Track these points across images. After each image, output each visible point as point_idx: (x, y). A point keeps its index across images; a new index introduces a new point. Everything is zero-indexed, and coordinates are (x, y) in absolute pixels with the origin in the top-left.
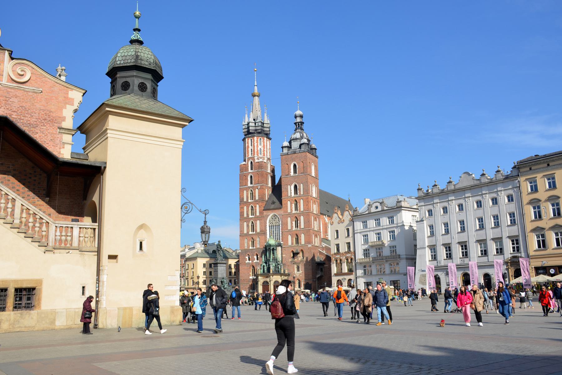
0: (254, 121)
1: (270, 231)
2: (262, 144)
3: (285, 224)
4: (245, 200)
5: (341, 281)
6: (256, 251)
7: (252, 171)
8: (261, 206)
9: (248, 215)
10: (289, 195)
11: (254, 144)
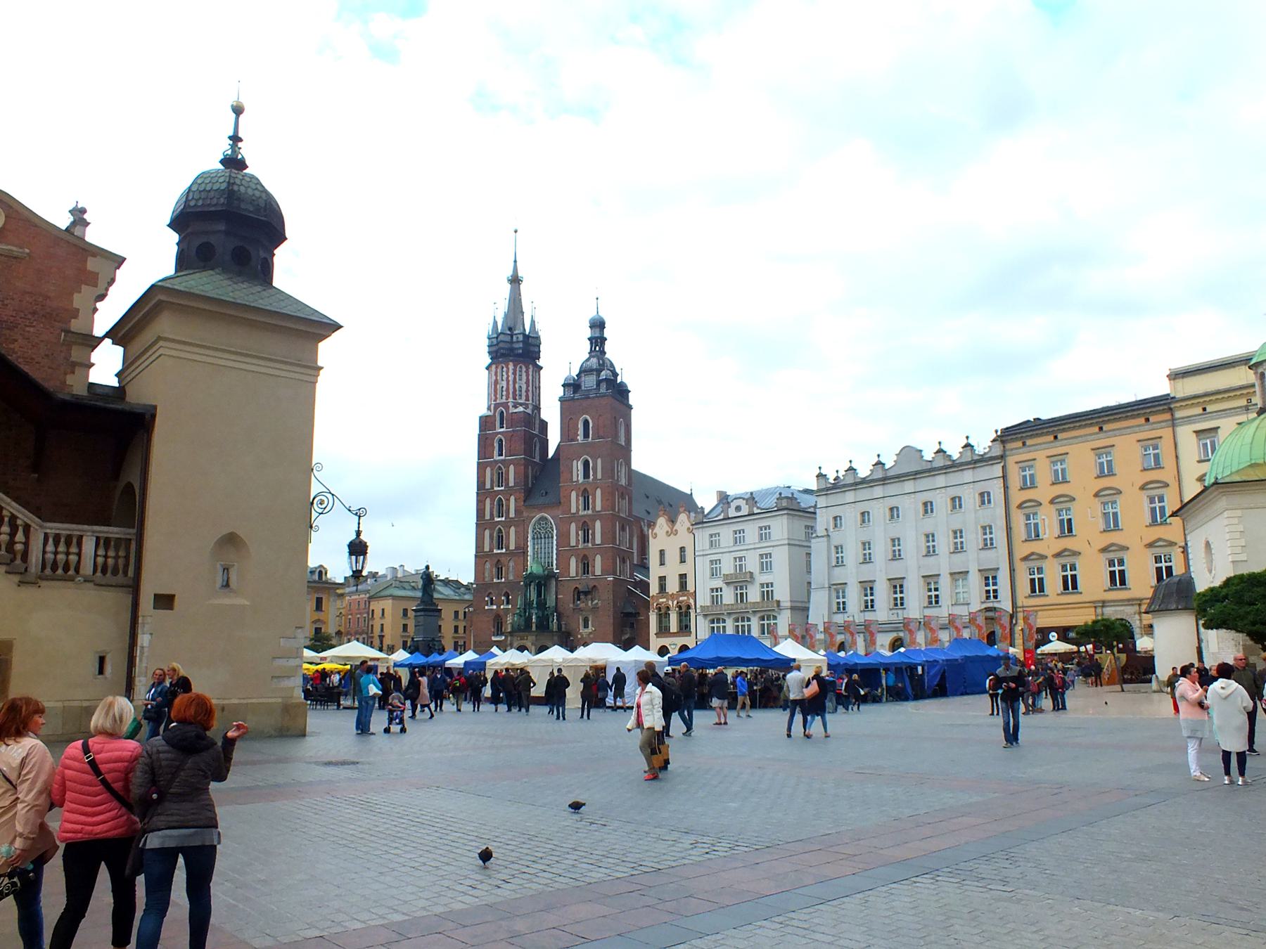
0: (509, 332)
1: (534, 548)
4: (488, 486)
5: (667, 647)
6: (506, 587)
7: (502, 430)
10: (575, 479)
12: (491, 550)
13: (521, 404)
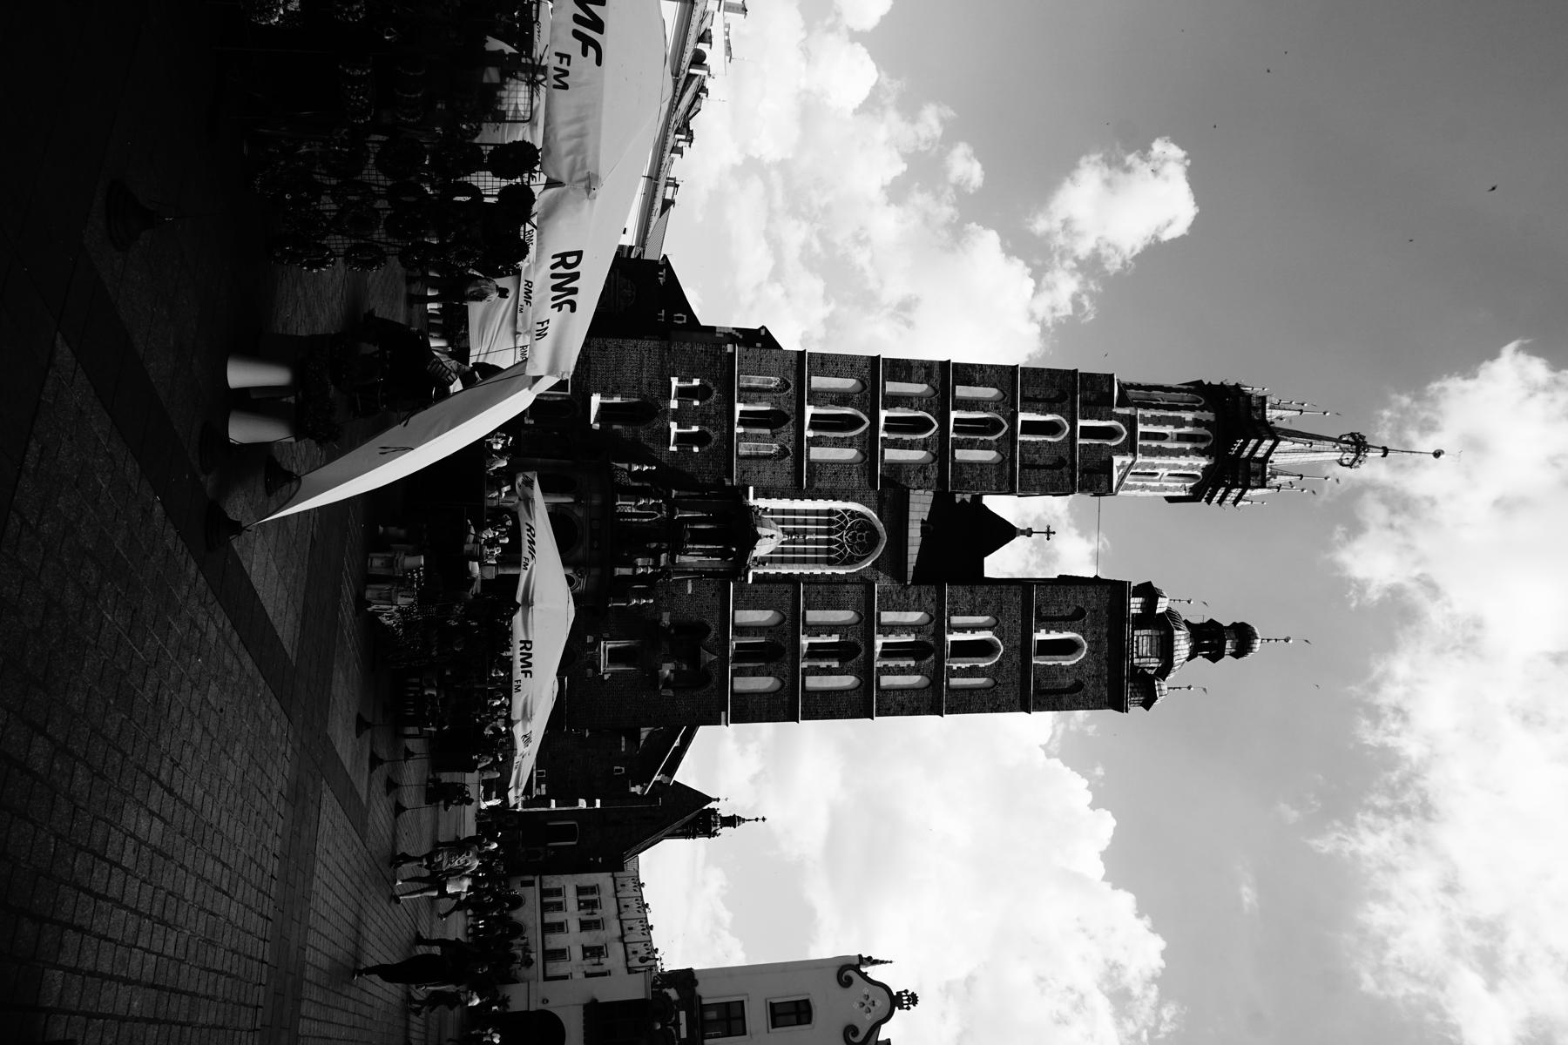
3: (828, 592)
8: (925, 478)
9: (894, 401)
10: (956, 620)
11: (1185, 453)
12: (818, 397)
13: (1123, 478)
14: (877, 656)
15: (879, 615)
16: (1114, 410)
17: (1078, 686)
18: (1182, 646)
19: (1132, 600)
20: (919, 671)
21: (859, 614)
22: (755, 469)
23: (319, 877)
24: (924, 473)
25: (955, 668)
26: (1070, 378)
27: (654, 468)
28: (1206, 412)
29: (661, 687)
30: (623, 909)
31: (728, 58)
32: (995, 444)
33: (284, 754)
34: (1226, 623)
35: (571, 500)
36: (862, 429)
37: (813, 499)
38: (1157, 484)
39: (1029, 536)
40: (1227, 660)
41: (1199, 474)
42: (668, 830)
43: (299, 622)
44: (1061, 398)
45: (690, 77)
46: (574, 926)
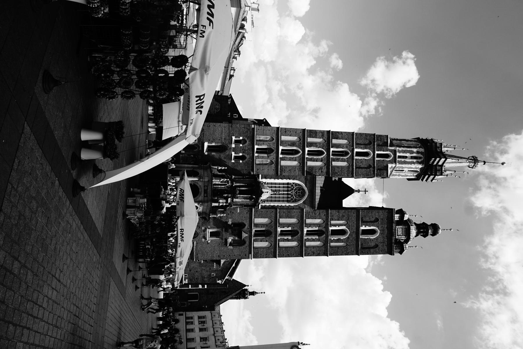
2: (409, 174)
3: (288, 212)
8: (322, 172)
9: (311, 144)
10: (333, 222)
11: (414, 163)
12: (284, 143)
13: (392, 172)
14: (305, 235)
15: (305, 220)
16: (388, 148)
17: (376, 246)
18: (413, 231)
19: (395, 215)
20: (319, 240)
21: (299, 220)
22: (262, 169)
23: (109, 312)
24: (321, 170)
25: (332, 239)
26: (373, 137)
27: (226, 168)
28: (421, 149)
29: (228, 245)
30: (214, 324)
31: (252, 26)
32: (347, 160)
33: (98, 268)
34: (429, 224)
35: (197, 179)
36: (299, 154)
37: (282, 179)
38: (404, 174)
39: (359, 192)
40: (429, 237)
41: (419, 170)
42: (231, 296)
43: (103, 222)
44: (370, 143)
45: (239, 33)
46: (197, 330)
